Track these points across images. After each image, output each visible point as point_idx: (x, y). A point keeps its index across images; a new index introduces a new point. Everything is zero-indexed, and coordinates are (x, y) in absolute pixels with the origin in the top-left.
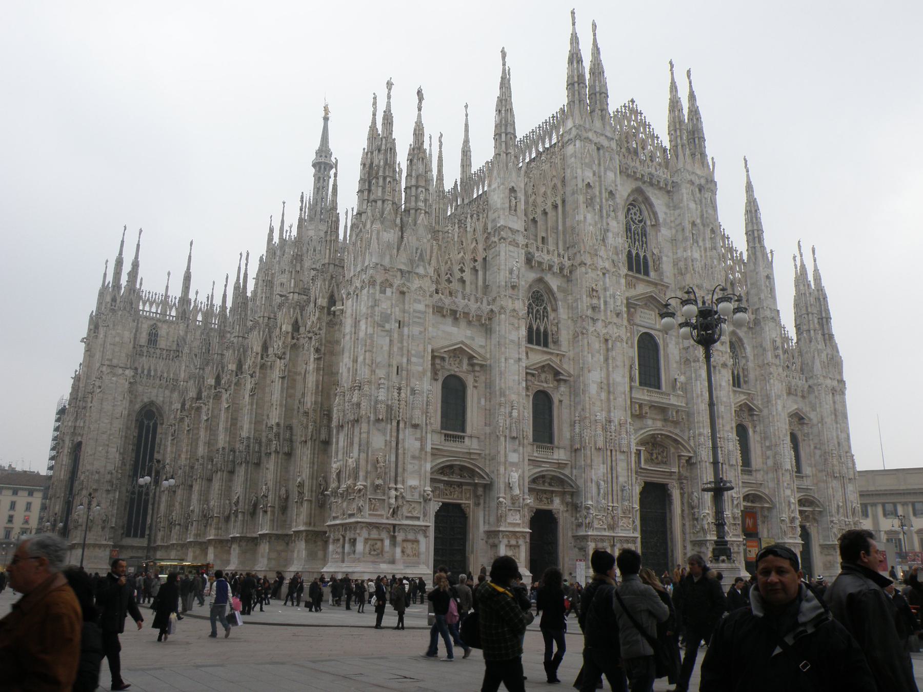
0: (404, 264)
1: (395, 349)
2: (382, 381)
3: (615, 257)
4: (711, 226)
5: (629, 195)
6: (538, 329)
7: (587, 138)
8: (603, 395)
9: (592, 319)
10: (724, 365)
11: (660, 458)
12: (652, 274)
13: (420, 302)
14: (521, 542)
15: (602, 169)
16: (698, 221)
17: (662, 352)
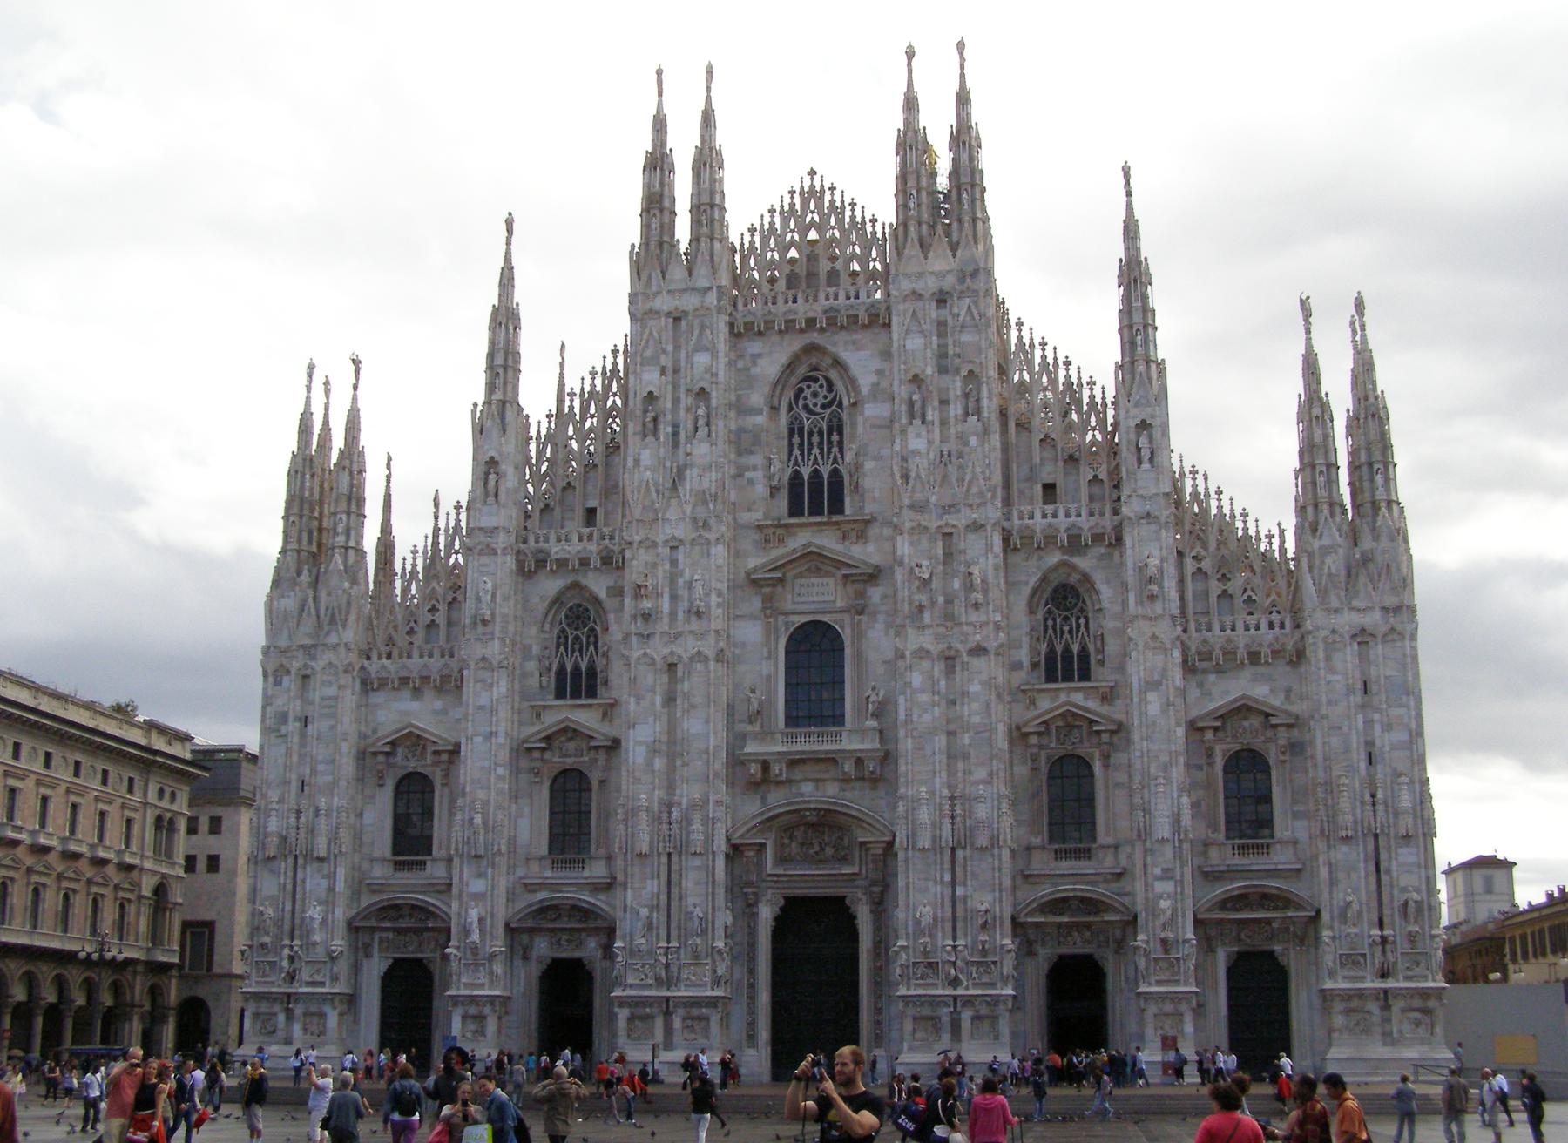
0: (309, 635)
1: (295, 758)
2: (275, 806)
3: (701, 512)
4: (964, 373)
5: (790, 367)
6: (576, 668)
7: (653, 313)
8: (659, 763)
9: (640, 635)
10: (979, 651)
11: (829, 851)
12: (847, 501)
13: (330, 684)
14: (487, 1010)
15: (683, 355)
16: (929, 371)
17: (848, 651)
